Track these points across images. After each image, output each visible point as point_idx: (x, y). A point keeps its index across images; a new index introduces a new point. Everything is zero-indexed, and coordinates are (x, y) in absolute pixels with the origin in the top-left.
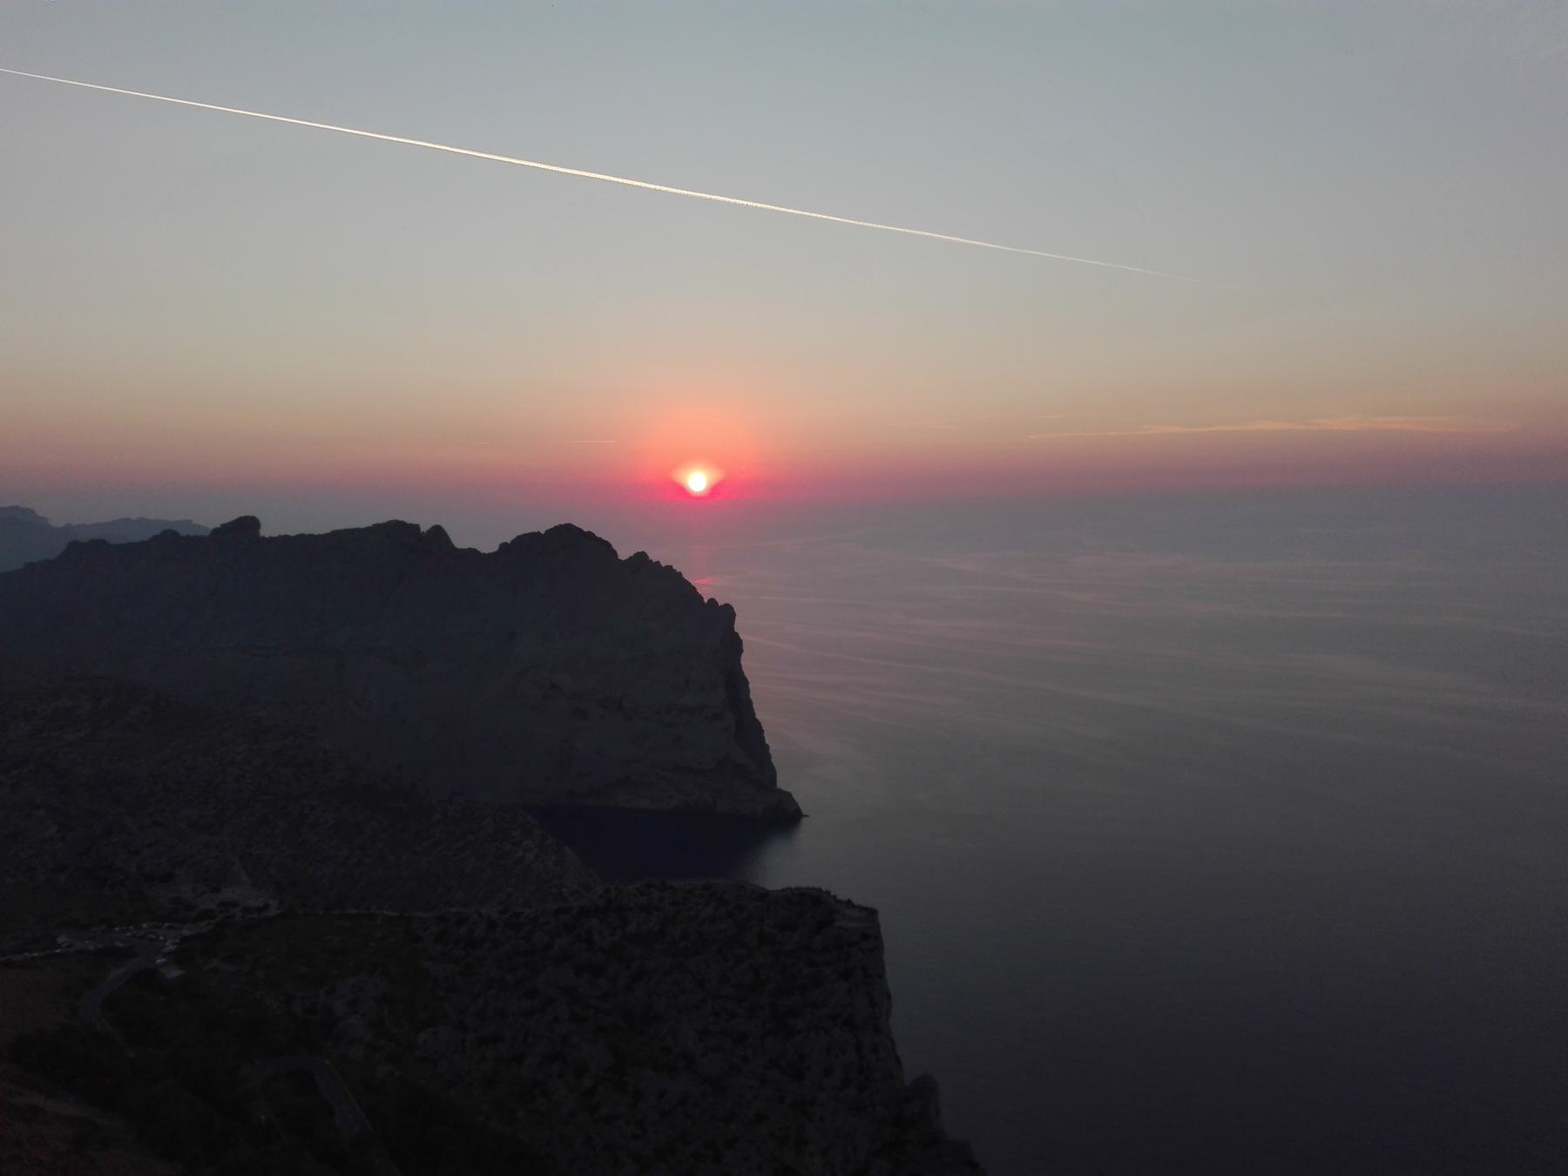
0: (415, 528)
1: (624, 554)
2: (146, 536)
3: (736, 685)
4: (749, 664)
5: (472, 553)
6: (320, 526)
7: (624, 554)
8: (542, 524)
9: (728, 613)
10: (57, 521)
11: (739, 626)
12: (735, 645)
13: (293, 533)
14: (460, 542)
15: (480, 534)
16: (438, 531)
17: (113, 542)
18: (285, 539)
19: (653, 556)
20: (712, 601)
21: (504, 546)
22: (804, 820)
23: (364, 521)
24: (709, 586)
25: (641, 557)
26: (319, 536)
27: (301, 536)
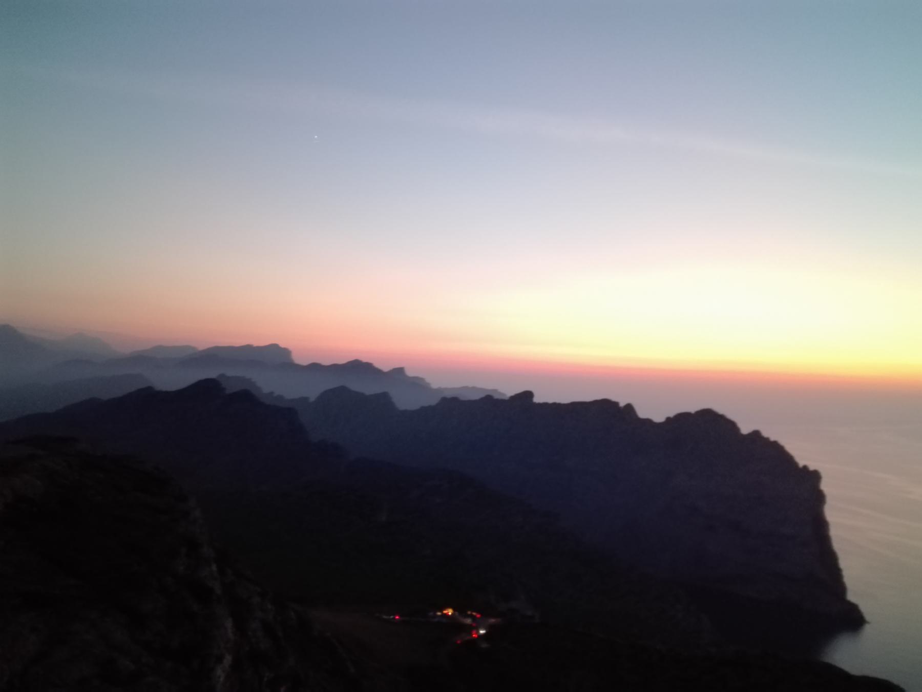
0: (616, 404)
1: (745, 429)
2: (476, 397)
3: (820, 526)
4: (831, 513)
5: (648, 422)
6: (565, 398)
7: (745, 429)
8: (693, 408)
9: (815, 476)
10: (434, 385)
11: (824, 486)
12: (820, 498)
13: (550, 401)
14: (642, 413)
15: (654, 410)
16: (629, 408)
17: (462, 398)
18: (545, 405)
19: (765, 433)
20: (805, 468)
21: (668, 419)
22: (867, 630)
23: (588, 398)
24: (804, 454)
25: (756, 434)
26: (564, 405)
27: (554, 404)
